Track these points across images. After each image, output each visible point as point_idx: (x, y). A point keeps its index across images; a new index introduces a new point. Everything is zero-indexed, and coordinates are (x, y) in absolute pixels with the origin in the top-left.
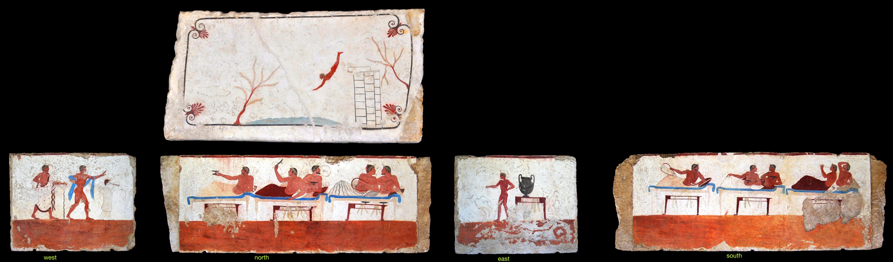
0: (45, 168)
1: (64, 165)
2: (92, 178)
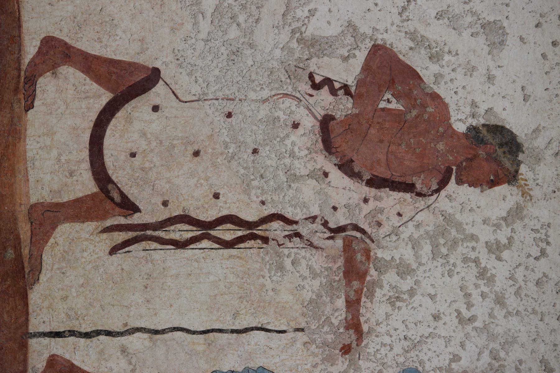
0: (492, 155)
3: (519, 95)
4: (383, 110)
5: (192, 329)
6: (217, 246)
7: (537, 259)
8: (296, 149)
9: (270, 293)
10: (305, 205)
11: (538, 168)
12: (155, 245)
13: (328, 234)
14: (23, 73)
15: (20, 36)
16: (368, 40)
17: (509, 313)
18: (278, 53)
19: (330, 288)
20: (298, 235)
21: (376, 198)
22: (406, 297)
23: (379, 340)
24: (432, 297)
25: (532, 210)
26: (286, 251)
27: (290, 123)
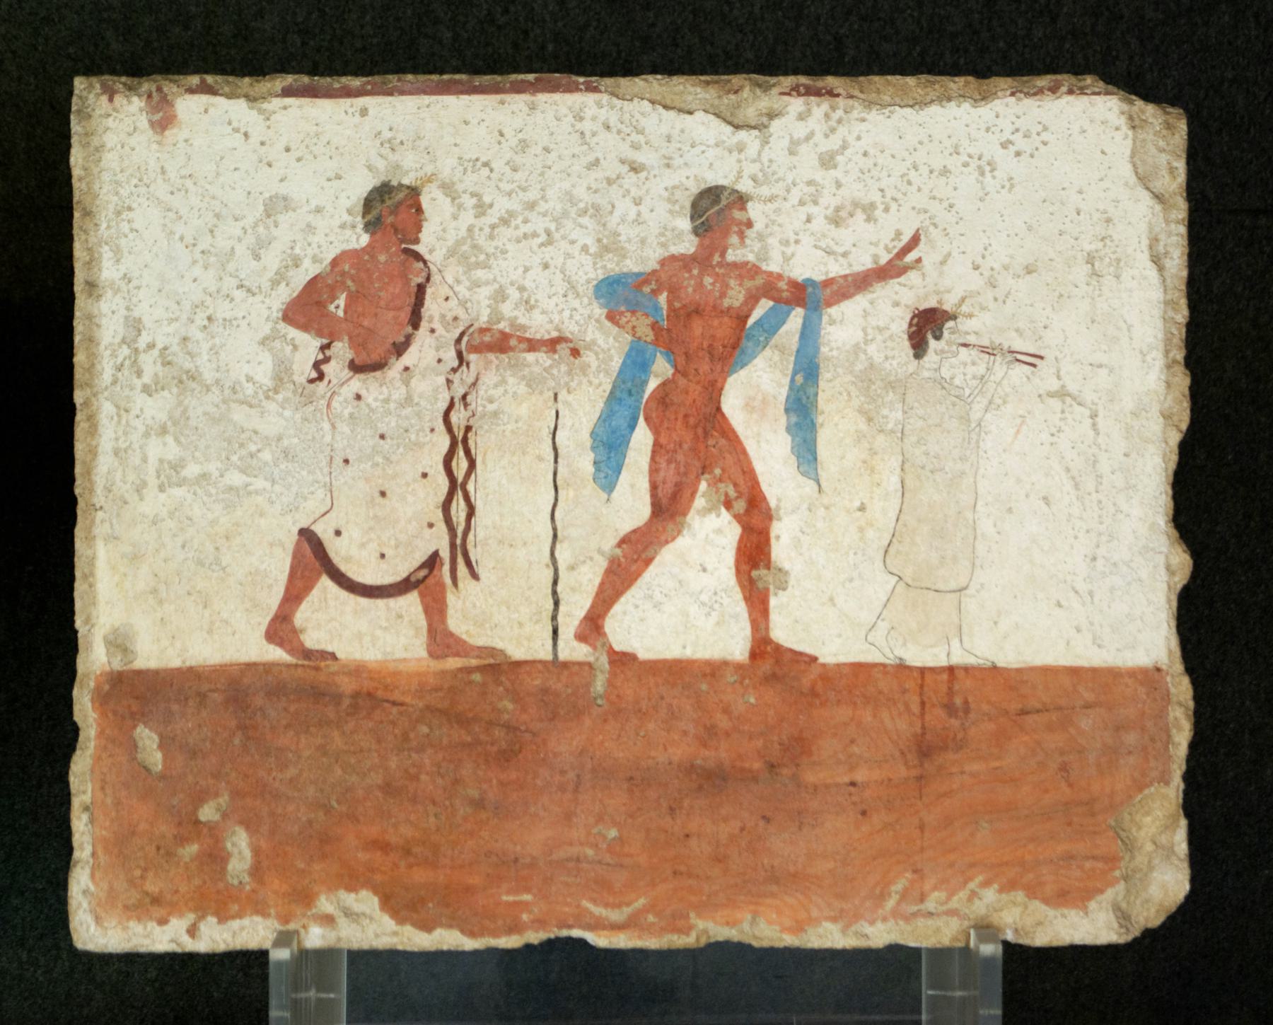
0: (392, 209)
1: (555, 180)
2: (800, 294)
3: (335, 183)
4: (345, 312)
7: (491, 170)
8: (381, 397)
9: (520, 424)
10: (436, 390)
11: (405, 168)
12: (471, 537)
13: (464, 368)
15: (264, 665)
16: (278, 326)
17: (542, 198)
18: (287, 413)
19: (516, 366)
20: (464, 397)
21: (430, 321)
22: (526, 295)
23: (566, 321)
24: (526, 270)
25: (446, 173)
26: (480, 409)
27: (356, 403)
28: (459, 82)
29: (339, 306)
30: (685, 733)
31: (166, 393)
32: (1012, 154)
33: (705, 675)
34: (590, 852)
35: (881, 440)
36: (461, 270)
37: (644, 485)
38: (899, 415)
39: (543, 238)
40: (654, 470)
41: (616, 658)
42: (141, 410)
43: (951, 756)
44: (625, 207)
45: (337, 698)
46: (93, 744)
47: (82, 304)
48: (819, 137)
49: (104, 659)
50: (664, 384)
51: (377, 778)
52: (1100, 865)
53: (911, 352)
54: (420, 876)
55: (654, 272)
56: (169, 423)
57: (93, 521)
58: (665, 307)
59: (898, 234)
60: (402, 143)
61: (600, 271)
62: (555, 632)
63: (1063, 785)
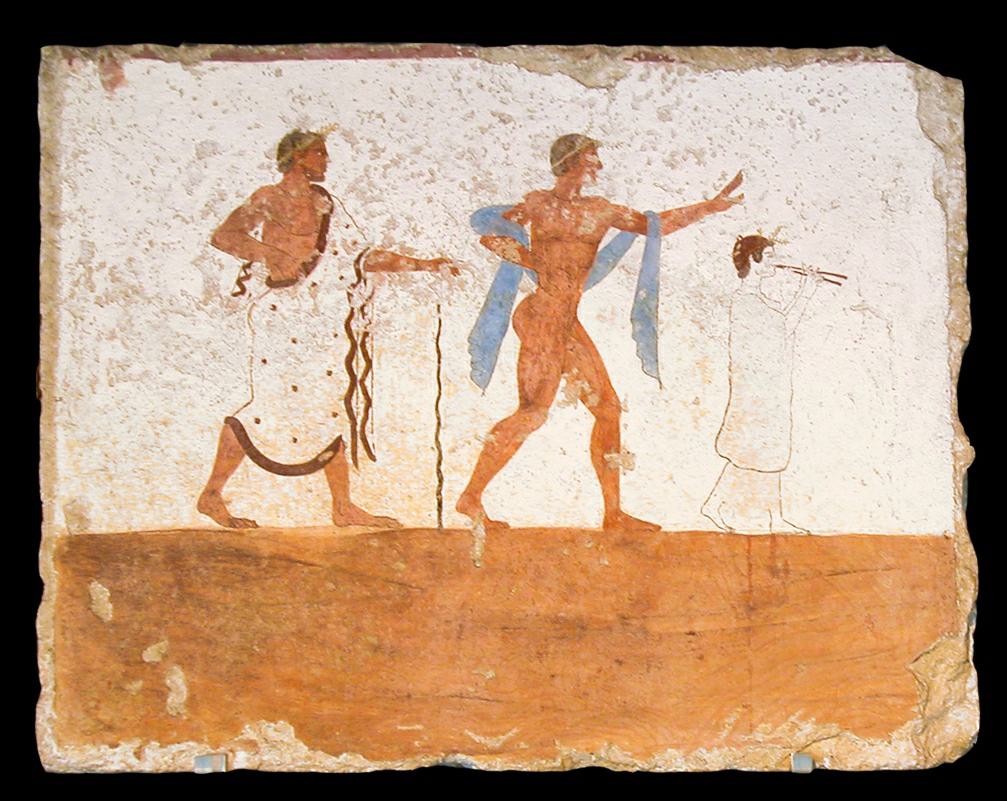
0: (302, 154)
2: (641, 224)
4: (263, 238)
5: (437, 395)
6: (370, 373)
8: (293, 308)
12: (368, 424)
13: (362, 284)
14: (227, 529)
15: (197, 531)
16: (207, 249)
17: (427, 143)
18: (215, 321)
19: (405, 283)
20: (362, 308)
21: (334, 245)
23: (447, 245)
25: (346, 126)
26: (376, 318)
28: (360, 49)
29: (257, 232)
30: (550, 590)
31: (114, 304)
32: (818, 110)
33: (566, 541)
34: (471, 689)
35: (711, 342)
36: (359, 203)
37: (514, 381)
38: (726, 324)
39: (428, 176)
40: (521, 369)
41: (491, 526)
42: (94, 318)
43: (775, 610)
44: (495, 151)
45: (256, 559)
46: (55, 595)
47: (46, 231)
48: (657, 95)
49: (64, 525)
50: (529, 298)
51: (291, 627)
52: (901, 701)
53: (736, 272)
54: (327, 709)
55: (520, 205)
56: (117, 329)
57: (54, 410)
58: (529, 233)
59: (724, 175)
60: (310, 98)
61: (474, 204)
62: (440, 504)
63: (869, 634)
